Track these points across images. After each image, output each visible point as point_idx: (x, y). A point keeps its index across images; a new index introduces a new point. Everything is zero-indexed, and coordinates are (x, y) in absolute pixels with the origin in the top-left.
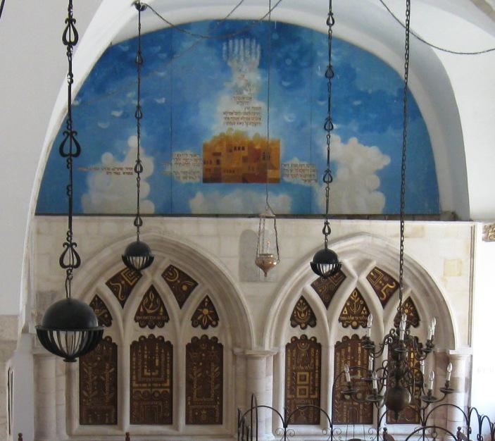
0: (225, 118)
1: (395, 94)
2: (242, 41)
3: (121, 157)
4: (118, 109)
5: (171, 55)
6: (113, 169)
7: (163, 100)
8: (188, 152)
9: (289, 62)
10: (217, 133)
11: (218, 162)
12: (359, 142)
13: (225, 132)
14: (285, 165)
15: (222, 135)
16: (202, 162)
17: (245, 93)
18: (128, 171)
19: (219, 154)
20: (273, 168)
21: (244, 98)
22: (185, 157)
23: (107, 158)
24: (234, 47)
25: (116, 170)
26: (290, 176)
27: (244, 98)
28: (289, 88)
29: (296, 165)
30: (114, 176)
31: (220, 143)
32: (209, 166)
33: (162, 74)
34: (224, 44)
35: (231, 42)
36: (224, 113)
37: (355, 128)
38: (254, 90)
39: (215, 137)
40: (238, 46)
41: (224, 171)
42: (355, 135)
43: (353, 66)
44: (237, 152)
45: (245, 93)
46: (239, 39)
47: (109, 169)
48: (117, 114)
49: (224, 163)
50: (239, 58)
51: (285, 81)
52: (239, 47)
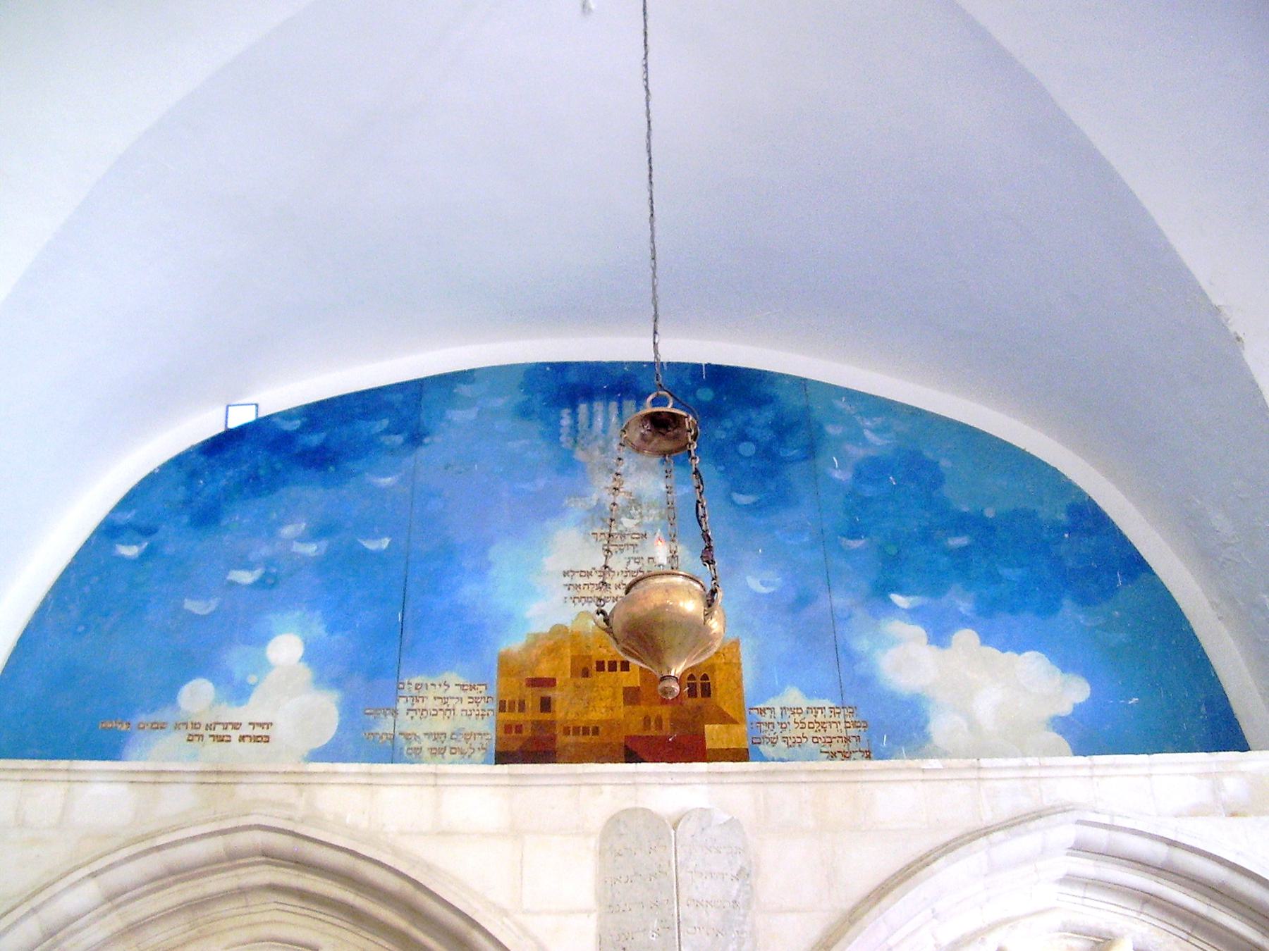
0: (569, 586)
1: (1062, 517)
2: (614, 405)
3: (240, 692)
4: (249, 567)
5: (416, 439)
6: (208, 727)
7: (385, 543)
8: (453, 678)
9: (747, 449)
10: (542, 627)
11: (546, 705)
12: (985, 641)
13: (569, 625)
14: (762, 711)
15: (558, 630)
16: (494, 706)
17: (627, 523)
18: (259, 731)
19: (551, 683)
20: (725, 719)
21: (623, 536)
22: (440, 692)
23: (197, 696)
24: (591, 416)
25: (219, 731)
26: (781, 744)
27: (623, 536)
28: (755, 508)
29: (796, 711)
30: (212, 747)
31: (553, 651)
32: (515, 717)
33: (387, 481)
34: (565, 412)
35: (583, 408)
36: (565, 574)
37: (965, 606)
38: (653, 516)
39: (536, 636)
40: (605, 418)
41: (566, 731)
42: (965, 622)
43: (929, 455)
44: (606, 675)
45: (627, 523)
46: (608, 400)
47: (196, 725)
48: (245, 577)
49: (566, 708)
50: (608, 442)
51: (740, 492)
52: (607, 420)
